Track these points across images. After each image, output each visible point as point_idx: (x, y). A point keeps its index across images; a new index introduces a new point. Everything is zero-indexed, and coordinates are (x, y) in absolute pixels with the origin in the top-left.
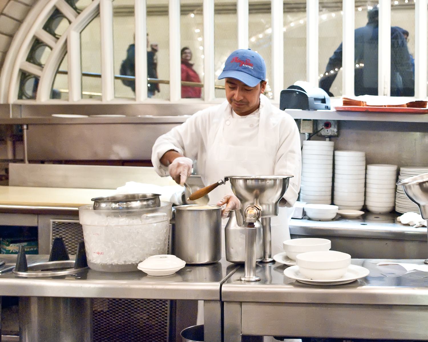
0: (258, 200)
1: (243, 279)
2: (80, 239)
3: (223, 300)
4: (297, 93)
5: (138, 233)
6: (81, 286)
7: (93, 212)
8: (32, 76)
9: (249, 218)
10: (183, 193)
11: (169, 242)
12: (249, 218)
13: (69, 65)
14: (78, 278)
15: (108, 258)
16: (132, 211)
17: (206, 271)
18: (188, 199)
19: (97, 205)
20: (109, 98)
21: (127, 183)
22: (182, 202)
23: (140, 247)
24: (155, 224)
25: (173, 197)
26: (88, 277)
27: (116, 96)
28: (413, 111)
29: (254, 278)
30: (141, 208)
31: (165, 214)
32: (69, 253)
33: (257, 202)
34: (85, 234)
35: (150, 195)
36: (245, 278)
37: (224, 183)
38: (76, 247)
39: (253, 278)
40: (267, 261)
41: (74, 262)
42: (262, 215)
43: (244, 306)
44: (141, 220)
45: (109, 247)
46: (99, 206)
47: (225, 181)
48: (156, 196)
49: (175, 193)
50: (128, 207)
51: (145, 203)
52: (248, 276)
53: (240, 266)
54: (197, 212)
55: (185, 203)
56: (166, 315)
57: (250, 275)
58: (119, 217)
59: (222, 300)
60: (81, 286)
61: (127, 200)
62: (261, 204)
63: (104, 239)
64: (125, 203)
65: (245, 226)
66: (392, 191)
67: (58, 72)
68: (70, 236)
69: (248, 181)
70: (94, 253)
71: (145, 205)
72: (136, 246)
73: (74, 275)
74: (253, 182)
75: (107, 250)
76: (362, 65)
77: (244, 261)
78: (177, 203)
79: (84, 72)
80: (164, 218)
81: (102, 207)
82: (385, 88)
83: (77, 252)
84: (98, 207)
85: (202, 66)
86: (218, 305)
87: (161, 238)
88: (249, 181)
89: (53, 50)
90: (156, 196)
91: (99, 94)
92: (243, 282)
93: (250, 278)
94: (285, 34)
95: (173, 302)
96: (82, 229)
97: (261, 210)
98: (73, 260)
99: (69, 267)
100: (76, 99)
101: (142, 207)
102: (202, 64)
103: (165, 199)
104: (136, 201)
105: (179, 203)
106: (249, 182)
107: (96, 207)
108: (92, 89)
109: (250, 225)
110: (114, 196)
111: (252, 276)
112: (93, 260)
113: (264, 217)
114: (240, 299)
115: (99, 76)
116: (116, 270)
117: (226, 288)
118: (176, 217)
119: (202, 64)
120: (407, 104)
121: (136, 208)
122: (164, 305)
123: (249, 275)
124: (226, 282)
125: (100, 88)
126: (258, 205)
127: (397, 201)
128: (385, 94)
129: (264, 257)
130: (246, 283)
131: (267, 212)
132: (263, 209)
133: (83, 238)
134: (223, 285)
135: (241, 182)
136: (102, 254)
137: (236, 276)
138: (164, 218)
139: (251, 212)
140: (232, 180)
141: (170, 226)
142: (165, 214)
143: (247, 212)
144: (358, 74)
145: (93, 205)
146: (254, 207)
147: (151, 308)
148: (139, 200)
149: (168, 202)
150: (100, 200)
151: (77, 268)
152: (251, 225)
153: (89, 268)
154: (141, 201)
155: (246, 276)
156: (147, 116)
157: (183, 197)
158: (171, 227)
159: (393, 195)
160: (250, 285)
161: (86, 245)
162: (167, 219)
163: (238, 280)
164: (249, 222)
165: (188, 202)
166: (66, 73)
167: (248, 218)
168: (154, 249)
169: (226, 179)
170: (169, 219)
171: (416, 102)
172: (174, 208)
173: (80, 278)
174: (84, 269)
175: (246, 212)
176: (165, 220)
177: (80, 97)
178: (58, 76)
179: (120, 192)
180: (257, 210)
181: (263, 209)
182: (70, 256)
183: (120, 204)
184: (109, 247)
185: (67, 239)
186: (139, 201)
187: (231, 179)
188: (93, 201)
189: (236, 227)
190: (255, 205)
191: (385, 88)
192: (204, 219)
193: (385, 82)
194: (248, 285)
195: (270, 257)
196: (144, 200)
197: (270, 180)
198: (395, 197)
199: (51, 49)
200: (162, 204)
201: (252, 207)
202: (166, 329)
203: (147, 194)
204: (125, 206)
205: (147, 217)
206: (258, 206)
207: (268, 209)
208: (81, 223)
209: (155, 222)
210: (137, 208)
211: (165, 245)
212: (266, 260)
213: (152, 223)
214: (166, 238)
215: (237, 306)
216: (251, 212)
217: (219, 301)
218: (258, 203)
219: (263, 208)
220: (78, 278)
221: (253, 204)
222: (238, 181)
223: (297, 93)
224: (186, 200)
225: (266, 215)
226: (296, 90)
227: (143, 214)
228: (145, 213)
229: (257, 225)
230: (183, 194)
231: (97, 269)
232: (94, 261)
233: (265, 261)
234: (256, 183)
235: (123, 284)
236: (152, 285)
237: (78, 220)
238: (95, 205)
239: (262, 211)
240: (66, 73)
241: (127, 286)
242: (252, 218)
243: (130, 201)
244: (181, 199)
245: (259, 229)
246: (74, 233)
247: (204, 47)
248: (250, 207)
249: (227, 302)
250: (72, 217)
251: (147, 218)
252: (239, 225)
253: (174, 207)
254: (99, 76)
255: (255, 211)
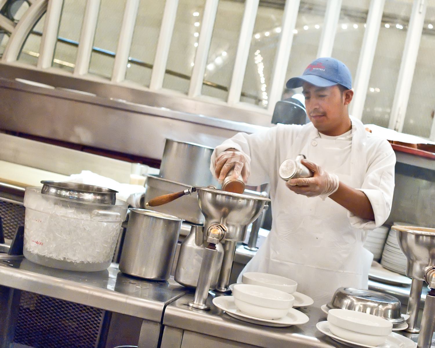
0: (225, 219)
1: (191, 305)
2: (19, 224)
3: (164, 323)
4: (295, 107)
5: (85, 229)
6: (12, 275)
7: (40, 195)
8: (3, 31)
9: (212, 238)
10: (142, 195)
11: (116, 247)
12: (212, 238)
13: (45, 28)
14: (10, 265)
15: (46, 251)
16: (84, 203)
17: (150, 289)
18: (147, 204)
19: (46, 189)
20: (82, 72)
21: (83, 172)
22: (139, 206)
23: (84, 245)
24: (105, 224)
25: (130, 197)
26: (21, 266)
27: (91, 70)
28: (421, 154)
29: (203, 307)
30: (93, 202)
31: (119, 214)
32: (6, 237)
33: (223, 222)
34: (27, 219)
35: (106, 190)
36: (194, 304)
37: (191, 193)
38: (14, 232)
39: (202, 306)
40: (223, 291)
41: (9, 247)
42: (227, 238)
43: (186, 336)
44: (91, 216)
45: (50, 239)
46: (48, 191)
47: (192, 192)
48: (112, 193)
49: (134, 194)
50: (79, 198)
51: (99, 197)
52: (197, 303)
53: (189, 291)
54: (155, 219)
55: (143, 207)
56: (97, 328)
57: (199, 302)
58: (68, 207)
59: (163, 322)
60: (12, 275)
61: (80, 190)
62: (227, 225)
63: (47, 229)
64: (76, 193)
65: (204, 246)
66: (381, 241)
67: (31, 32)
68: (9, 218)
69: (218, 196)
70: (33, 241)
71: (98, 200)
72: (80, 243)
73: (6, 261)
74: (224, 198)
75: (47, 241)
76: (378, 90)
77: (196, 286)
78: (134, 206)
79: (60, 37)
80: (117, 219)
81: (51, 192)
82: (397, 122)
83: (15, 237)
84: (47, 191)
85: (193, 56)
86: (157, 329)
87: (109, 241)
88: (219, 197)
89: (32, 6)
90: (112, 193)
91: (72, 65)
92: (190, 308)
93: (199, 305)
94: (295, 37)
95: (108, 314)
96: (24, 213)
97: (226, 232)
98: (8, 244)
99: (2, 251)
100: (45, 66)
101: (95, 201)
102: (193, 53)
103: (122, 196)
104: (90, 193)
105: (136, 206)
106: (219, 198)
107: (44, 190)
108: (64, 57)
109: (211, 246)
110: (66, 183)
111: (201, 304)
112: (29, 249)
113: (228, 240)
114: (183, 327)
115: (76, 45)
116: (53, 265)
117: (169, 310)
118: (130, 220)
119: (193, 53)
120: (418, 145)
121: (88, 201)
122: (97, 317)
123: (198, 302)
124: (171, 304)
125: (74, 59)
126: (224, 225)
127: (384, 253)
128: (397, 128)
129: (219, 285)
130: (194, 310)
131: (232, 235)
132: (229, 231)
133: (24, 223)
134: (167, 307)
135: (209, 196)
136: (41, 244)
137: (183, 300)
138: (116, 219)
139: (214, 231)
140: (200, 192)
141: (121, 230)
142: (119, 214)
143: (210, 230)
144: (370, 99)
145: (42, 188)
146: (219, 227)
147: (83, 317)
148: (93, 193)
149: (124, 202)
150: (49, 184)
151: (10, 255)
152: (212, 246)
153: (24, 257)
154: (95, 194)
155: (195, 302)
156: (120, 101)
157: (143, 200)
158: (122, 231)
159: (380, 246)
160: (198, 312)
161: (26, 231)
162: (120, 221)
163: (185, 305)
164: (210, 242)
165: (147, 207)
166: (39, 34)
167: (210, 237)
168: (98, 251)
169: (194, 190)
170: (123, 221)
171: (428, 144)
172: (129, 209)
173: (12, 265)
174: (17, 256)
175: (209, 230)
176: (117, 221)
177: (50, 65)
178: (32, 36)
179: (73, 179)
180: (222, 230)
181: (229, 231)
182: (6, 240)
183: (71, 192)
184: (50, 239)
185: (5, 221)
186: (92, 194)
187: (199, 191)
188: (42, 183)
189: (194, 246)
190: (220, 224)
191: (397, 122)
192: (160, 228)
193: (398, 114)
194: (195, 312)
195: (226, 287)
196: (99, 194)
197: (243, 199)
198: (383, 249)
199: (30, 4)
200: (117, 203)
201: (217, 226)
202: (94, 344)
203: (102, 188)
204: (76, 196)
205: (98, 213)
206: (225, 227)
207: (234, 232)
208: (25, 204)
209: (106, 221)
210: (89, 202)
211: (111, 248)
212: (221, 289)
213: (102, 222)
214: (114, 242)
215: (177, 334)
216: (215, 232)
217: (159, 323)
218: (225, 223)
219: (229, 230)
220: (10, 265)
221: (219, 223)
222: (206, 194)
223: (295, 107)
224: (145, 205)
225: (232, 239)
226: (294, 104)
227: (94, 209)
228: (97, 209)
229: (219, 247)
230: (144, 196)
231: (33, 260)
232: (31, 250)
233: (220, 291)
234: (227, 199)
235: (58, 282)
236: (89, 290)
237: (23, 202)
238: (44, 189)
239: (227, 233)
240: (39, 34)
241: (61, 285)
242: (215, 238)
243: (83, 192)
244: (139, 201)
245: (220, 254)
246: (14, 215)
247: (199, 34)
248: (214, 226)
249: (168, 326)
250: (15, 197)
251: (98, 215)
252: (198, 245)
253: (130, 208)
254: (76, 45)
255: (219, 231)
